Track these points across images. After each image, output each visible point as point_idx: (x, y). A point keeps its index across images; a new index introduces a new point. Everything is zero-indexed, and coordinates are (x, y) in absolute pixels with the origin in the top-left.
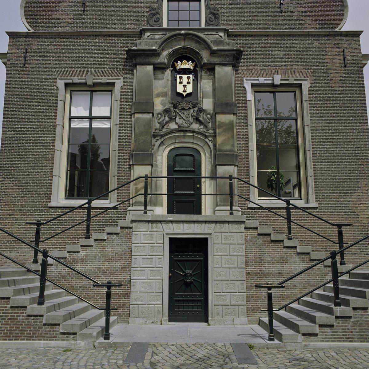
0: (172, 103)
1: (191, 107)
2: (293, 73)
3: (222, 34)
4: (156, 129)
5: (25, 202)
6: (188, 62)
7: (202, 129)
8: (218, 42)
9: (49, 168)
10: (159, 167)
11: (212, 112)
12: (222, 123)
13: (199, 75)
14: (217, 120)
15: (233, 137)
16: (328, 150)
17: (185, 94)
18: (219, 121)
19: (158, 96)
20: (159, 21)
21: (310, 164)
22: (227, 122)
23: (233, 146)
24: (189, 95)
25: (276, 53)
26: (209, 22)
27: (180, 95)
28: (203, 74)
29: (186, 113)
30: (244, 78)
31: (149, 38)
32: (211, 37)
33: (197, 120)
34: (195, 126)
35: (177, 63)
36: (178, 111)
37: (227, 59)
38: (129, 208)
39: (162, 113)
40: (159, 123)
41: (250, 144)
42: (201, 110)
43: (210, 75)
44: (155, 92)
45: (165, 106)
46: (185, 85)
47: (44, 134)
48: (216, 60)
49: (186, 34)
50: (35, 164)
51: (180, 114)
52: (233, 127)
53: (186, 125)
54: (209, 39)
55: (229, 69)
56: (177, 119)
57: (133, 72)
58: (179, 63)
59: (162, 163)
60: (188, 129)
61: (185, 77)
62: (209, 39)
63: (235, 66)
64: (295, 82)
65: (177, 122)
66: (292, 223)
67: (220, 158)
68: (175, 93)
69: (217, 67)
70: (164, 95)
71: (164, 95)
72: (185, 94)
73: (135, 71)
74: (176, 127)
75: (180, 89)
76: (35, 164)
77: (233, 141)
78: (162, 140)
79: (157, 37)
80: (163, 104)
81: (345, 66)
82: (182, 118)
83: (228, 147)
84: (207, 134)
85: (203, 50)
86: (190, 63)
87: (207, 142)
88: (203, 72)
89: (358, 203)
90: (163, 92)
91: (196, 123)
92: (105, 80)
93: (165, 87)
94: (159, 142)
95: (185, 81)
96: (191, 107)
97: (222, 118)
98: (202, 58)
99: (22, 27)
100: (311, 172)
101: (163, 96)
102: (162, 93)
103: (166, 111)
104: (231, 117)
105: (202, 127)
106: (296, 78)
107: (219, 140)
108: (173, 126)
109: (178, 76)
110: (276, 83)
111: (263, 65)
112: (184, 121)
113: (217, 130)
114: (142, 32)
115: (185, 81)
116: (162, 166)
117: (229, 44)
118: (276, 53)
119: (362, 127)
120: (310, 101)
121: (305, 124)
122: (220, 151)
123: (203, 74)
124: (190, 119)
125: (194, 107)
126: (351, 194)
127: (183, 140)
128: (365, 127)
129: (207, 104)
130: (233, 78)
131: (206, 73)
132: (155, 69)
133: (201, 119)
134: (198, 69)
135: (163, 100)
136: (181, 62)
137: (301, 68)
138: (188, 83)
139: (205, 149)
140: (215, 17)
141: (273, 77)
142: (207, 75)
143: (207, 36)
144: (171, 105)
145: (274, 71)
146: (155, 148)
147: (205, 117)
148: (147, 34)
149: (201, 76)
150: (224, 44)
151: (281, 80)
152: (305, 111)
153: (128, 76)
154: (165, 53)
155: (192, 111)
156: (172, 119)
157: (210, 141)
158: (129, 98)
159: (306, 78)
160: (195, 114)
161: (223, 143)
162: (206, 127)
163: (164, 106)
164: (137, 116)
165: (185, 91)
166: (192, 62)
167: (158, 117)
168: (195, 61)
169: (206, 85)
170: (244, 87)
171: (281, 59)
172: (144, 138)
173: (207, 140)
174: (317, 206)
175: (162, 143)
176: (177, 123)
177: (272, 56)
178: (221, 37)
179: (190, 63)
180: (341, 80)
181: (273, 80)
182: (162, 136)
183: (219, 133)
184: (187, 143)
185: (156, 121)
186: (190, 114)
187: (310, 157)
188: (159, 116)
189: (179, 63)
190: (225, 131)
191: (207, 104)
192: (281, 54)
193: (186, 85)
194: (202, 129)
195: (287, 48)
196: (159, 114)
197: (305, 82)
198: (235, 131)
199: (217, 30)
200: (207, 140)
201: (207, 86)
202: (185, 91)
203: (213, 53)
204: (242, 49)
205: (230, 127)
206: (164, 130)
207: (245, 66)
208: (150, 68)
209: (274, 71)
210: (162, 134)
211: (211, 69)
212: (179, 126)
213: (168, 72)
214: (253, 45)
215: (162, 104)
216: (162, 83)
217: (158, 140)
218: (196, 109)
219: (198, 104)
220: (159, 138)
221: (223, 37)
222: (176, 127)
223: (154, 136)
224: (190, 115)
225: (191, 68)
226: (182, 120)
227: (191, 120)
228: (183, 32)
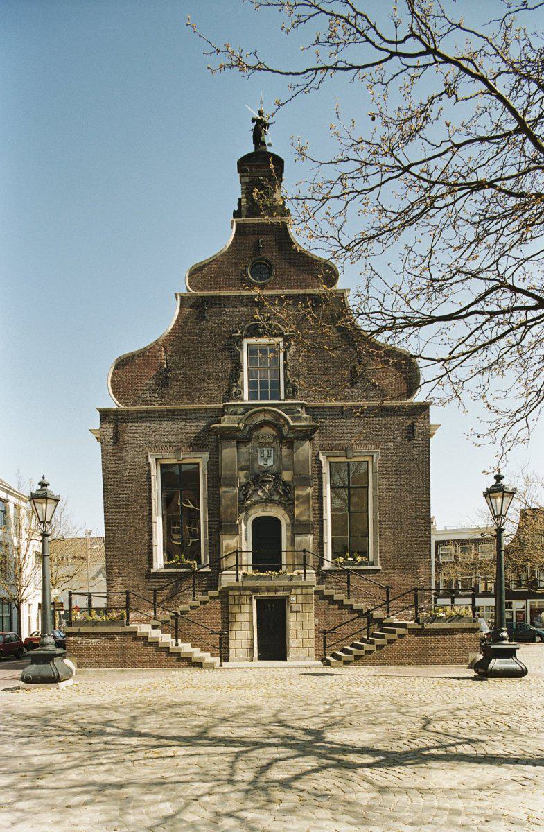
15: (309, 508)
30: (320, 452)
38: (223, 573)
43: (288, 448)
67: (298, 527)
79: (239, 412)
83: (304, 518)
93: (248, 460)
99: (112, 403)
102: (245, 466)
107: (297, 511)
122: (297, 521)
132: (238, 443)
161: (301, 514)
172: (230, 511)
190: (302, 503)
198: (311, 503)
205: (306, 499)
215: (245, 477)
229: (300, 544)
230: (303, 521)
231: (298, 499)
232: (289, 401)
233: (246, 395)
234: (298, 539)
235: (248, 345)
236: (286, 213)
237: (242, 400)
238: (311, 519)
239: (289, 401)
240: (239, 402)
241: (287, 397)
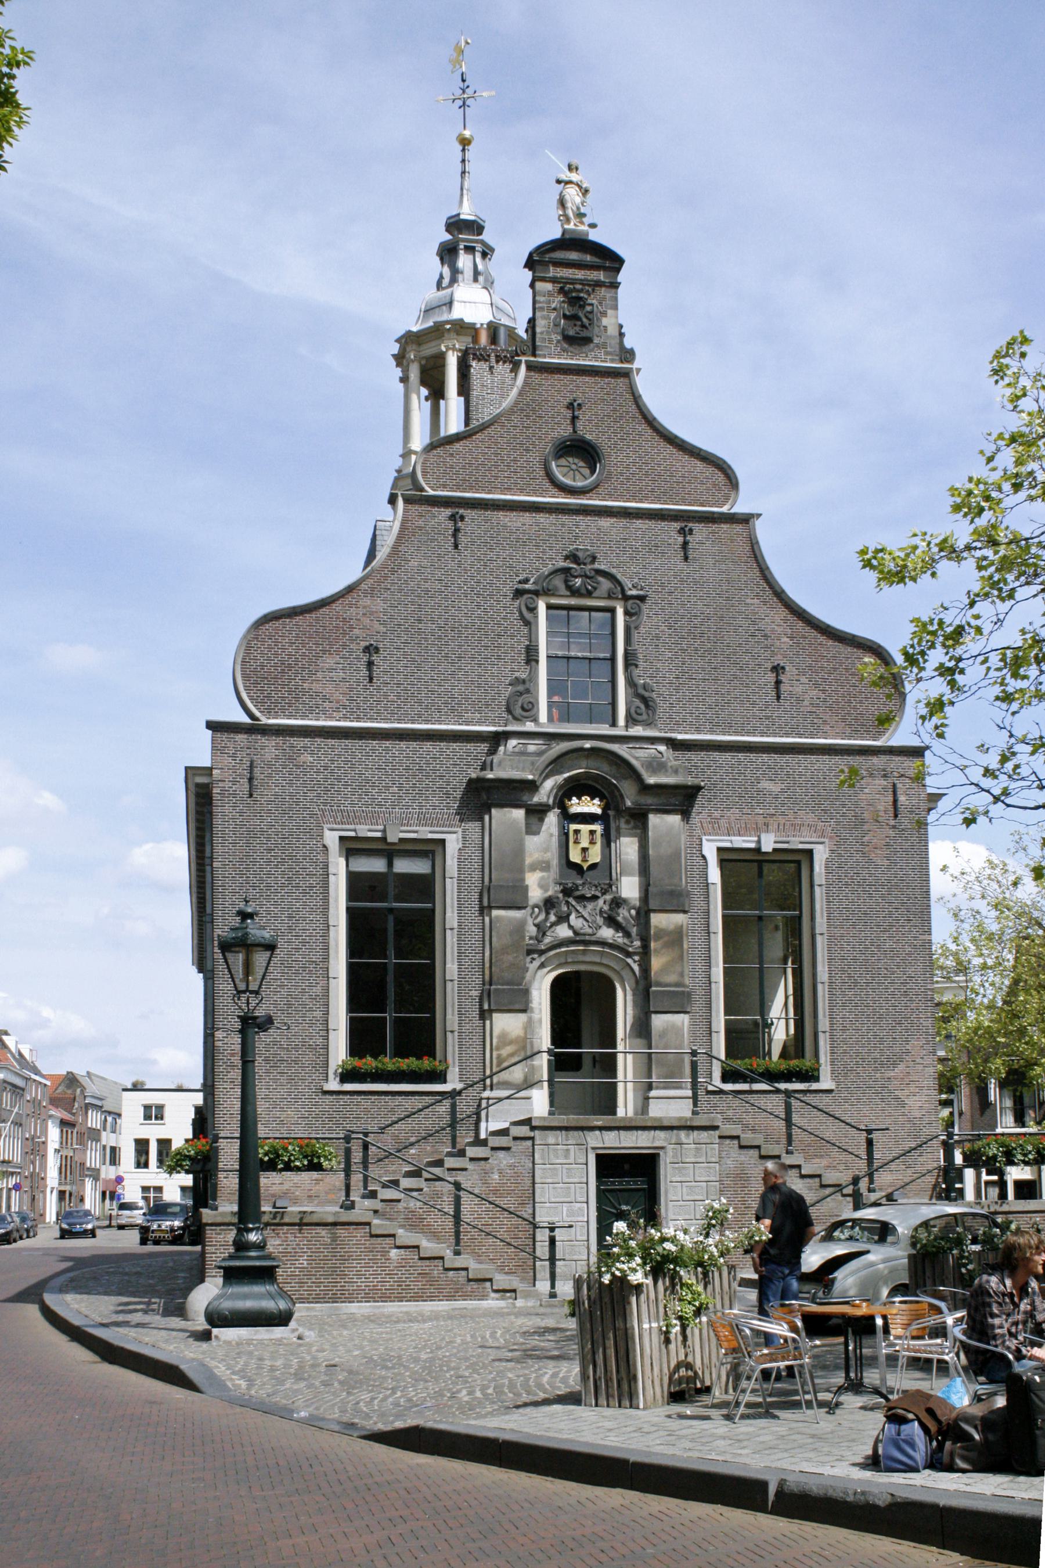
0: (560, 884)
1: (599, 895)
2: (796, 827)
3: (662, 748)
4: (531, 938)
5: (275, 1080)
6: (592, 799)
7: (619, 938)
8: (655, 765)
9: (318, 1014)
10: (537, 1011)
11: (638, 904)
12: (662, 930)
13: (613, 825)
14: (652, 924)
15: (681, 957)
16: (856, 983)
17: (585, 866)
18: (656, 927)
19: (533, 868)
20: (529, 710)
21: (824, 1009)
22: (672, 927)
23: (682, 975)
24: (593, 866)
25: (765, 784)
26: (635, 716)
27: (577, 868)
28: (623, 825)
29: (590, 906)
31: (516, 750)
32: (640, 753)
33: (611, 921)
34: (607, 933)
35: (570, 800)
36: (574, 903)
37: (673, 800)
39: (541, 904)
40: (535, 925)
41: (713, 969)
42: (618, 902)
43: (635, 827)
44: (528, 861)
45: (546, 891)
46: (587, 846)
47: (304, 943)
48: (649, 800)
49: (592, 749)
50: (289, 1005)
51: (578, 908)
52: (682, 938)
53: (590, 931)
54: (637, 758)
55: (675, 819)
56: (572, 917)
57: (482, 820)
58: (575, 800)
59: (540, 1004)
60: (593, 938)
61: (585, 828)
62: (637, 758)
63: (686, 814)
64: (801, 846)
65: (572, 923)
66: (784, 1117)
68: (564, 862)
69: (651, 816)
70: (544, 866)
71: (544, 866)
72: (585, 866)
73: (487, 817)
74: (570, 933)
75: (575, 857)
76: (289, 1005)
77: (683, 966)
78: (543, 959)
79: (531, 748)
80: (543, 886)
81: (896, 816)
82: (582, 916)
83: (672, 978)
84: (630, 949)
85: (626, 779)
86: (597, 801)
87: (628, 965)
88: (623, 820)
89: (907, 1081)
90: (544, 862)
91: (609, 926)
92: (426, 833)
93: (546, 850)
94: (536, 963)
95: (585, 843)
96: (599, 895)
97: (658, 920)
98: (622, 796)
100: (824, 1024)
101: (542, 870)
103: (549, 904)
104: (679, 918)
105: (620, 935)
106: (802, 839)
108: (563, 932)
109: (573, 827)
110: (764, 850)
111: (741, 809)
112: (585, 923)
113: (652, 945)
114: (497, 739)
115: (585, 843)
116: (541, 1010)
117: (676, 772)
118: (765, 784)
119: (922, 937)
120: (828, 885)
121: (817, 932)
123: (623, 825)
124: (598, 917)
125: (603, 894)
126: (895, 1065)
127: (581, 958)
128: (926, 937)
129: (629, 888)
130: (683, 838)
131: (627, 822)
133: (620, 919)
134: (611, 813)
135: (542, 878)
136: (579, 798)
137: (811, 818)
138: (592, 842)
139: (625, 977)
140: (647, 706)
141: (759, 837)
142: (630, 826)
143: (633, 751)
144: (558, 888)
145: (760, 820)
146: (528, 975)
147: (626, 914)
148: (512, 743)
149: (618, 829)
150: (666, 771)
151: (775, 842)
152: (818, 906)
153: (473, 826)
154: (549, 784)
155: (601, 902)
156: (563, 919)
157: (635, 962)
158: (477, 875)
159: (822, 840)
160: (606, 908)
162: (627, 934)
163: (546, 891)
164: (495, 913)
165: (584, 860)
166: (601, 800)
167: (533, 912)
168: (605, 797)
169: (628, 847)
170: (704, 857)
171: (776, 798)
173: (629, 961)
174: (833, 1087)
175: (542, 966)
176: (570, 927)
177: (759, 791)
178: (661, 753)
179: (597, 801)
180: (887, 845)
181: (759, 842)
182: (542, 953)
183: (655, 950)
184: (590, 961)
185: (530, 921)
186: (598, 909)
187: (824, 996)
188: (536, 910)
189: (575, 800)
191: (629, 888)
192: (775, 788)
193: (587, 849)
194: (619, 938)
195: (788, 775)
196: (536, 906)
197: (820, 847)
198: (685, 946)
199: (653, 740)
200: (629, 961)
201: (629, 850)
202: (584, 860)
203: (645, 789)
204: (702, 784)
205: (675, 938)
206: (547, 940)
207: (704, 814)
208: (519, 814)
209: (760, 820)
210: (543, 947)
211: (639, 819)
212: (576, 933)
213: (552, 819)
214: (721, 767)
216: (542, 843)
217: (533, 959)
218: (608, 897)
219: (611, 886)
220: (535, 956)
221: (665, 755)
222: (570, 933)
223: (529, 952)
224: (598, 911)
225: (599, 811)
226: (581, 920)
227: (600, 920)
228: (588, 745)
229: (663, 1034)
230: (667, 985)
231: (658, 937)
232: (638, 731)
233: (543, 717)
234: (658, 1021)
235: (549, 607)
236: (628, 355)
237: (535, 720)
238: (687, 981)
239: (638, 731)
240: (530, 727)
241: (632, 720)
